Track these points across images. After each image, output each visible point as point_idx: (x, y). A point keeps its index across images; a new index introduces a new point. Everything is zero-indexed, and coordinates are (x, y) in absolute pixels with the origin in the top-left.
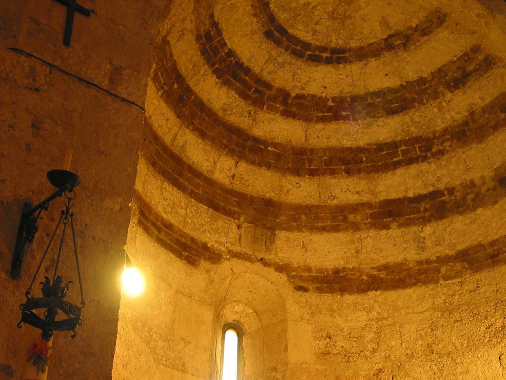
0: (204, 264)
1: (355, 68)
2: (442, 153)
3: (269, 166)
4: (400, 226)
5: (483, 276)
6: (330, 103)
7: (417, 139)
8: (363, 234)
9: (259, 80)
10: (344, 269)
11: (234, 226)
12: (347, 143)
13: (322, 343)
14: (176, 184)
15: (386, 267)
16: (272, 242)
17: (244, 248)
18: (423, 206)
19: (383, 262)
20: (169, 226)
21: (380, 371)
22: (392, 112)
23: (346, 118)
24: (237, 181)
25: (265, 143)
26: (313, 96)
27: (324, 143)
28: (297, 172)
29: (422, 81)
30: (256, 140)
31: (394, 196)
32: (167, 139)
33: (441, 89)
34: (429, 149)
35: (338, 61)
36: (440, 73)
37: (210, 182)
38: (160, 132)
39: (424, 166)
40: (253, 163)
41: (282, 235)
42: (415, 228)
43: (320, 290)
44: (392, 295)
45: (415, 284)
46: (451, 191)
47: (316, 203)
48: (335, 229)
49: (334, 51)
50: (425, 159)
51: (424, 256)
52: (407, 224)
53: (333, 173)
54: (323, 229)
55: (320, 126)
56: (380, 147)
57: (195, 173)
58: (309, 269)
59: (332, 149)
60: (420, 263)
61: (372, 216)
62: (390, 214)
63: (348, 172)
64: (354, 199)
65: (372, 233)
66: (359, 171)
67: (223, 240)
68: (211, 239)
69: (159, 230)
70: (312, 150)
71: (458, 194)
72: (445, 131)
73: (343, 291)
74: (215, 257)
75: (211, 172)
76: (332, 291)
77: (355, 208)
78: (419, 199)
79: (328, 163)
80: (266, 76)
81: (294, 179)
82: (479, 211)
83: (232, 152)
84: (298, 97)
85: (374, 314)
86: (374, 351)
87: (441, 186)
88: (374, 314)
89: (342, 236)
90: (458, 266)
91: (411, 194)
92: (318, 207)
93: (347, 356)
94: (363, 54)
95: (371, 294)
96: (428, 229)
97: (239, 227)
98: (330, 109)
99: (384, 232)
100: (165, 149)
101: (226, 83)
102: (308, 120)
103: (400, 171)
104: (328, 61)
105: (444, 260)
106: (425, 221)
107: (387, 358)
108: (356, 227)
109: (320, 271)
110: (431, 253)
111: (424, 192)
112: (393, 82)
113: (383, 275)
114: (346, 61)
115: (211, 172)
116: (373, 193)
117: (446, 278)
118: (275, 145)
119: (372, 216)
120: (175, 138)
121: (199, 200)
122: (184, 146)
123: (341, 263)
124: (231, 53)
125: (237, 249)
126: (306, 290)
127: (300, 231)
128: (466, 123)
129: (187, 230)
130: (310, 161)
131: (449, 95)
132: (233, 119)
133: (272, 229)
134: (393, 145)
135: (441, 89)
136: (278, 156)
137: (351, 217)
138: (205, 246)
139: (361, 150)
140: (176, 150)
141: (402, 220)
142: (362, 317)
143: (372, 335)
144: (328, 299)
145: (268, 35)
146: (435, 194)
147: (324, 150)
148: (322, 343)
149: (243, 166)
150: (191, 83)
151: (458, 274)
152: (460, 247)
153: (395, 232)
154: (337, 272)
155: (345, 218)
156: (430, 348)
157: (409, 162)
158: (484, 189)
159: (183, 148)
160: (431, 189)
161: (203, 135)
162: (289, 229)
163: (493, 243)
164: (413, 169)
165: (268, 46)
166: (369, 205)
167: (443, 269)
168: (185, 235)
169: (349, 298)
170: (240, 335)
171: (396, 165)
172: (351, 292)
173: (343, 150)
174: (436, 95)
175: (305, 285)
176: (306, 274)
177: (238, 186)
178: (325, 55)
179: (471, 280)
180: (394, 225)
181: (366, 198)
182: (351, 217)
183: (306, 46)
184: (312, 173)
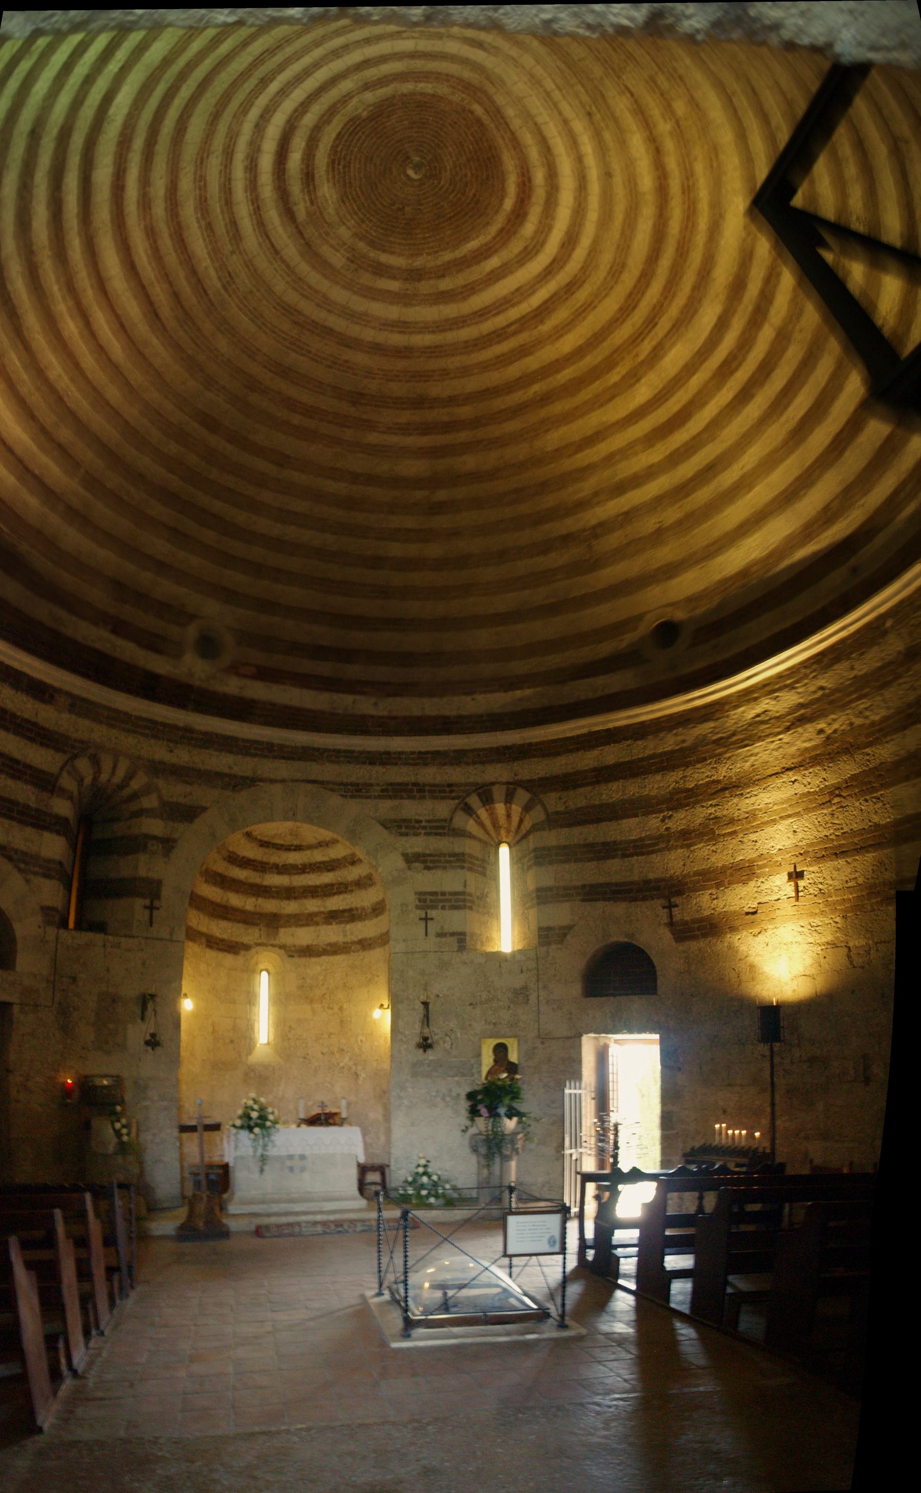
0: (243, 952)
1: (308, 852)
2: (352, 891)
3: (273, 897)
4: (337, 923)
5: (366, 953)
6: (300, 866)
7: (341, 884)
8: (320, 927)
9: (262, 863)
10: (311, 945)
11: (257, 930)
12: (311, 883)
13: (301, 982)
14: (226, 919)
15: (330, 944)
16: (277, 934)
17: (263, 940)
18: (346, 914)
19: (328, 941)
20: (223, 940)
21: (325, 994)
22: (329, 871)
23: (308, 873)
24: (258, 908)
25: (270, 887)
26: (291, 864)
27: (300, 884)
28: (288, 898)
29: (338, 860)
30: (266, 887)
31: (334, 908)
32: (218, 900)
33: (347, 865)
34: (346, 888)
35: (300, 850)
36: (344, 858)
37: (243, 912)
38: (214, 899)
39: (346, 896)
40: (265, 897)
41: (282, 931)
42: (343, 925)
43: (300, 956)
44: (332, 958)
45: (341, 953)
46: (357, 909)
47: (297, 912)
48: (307, 925)
49: (296, 846)
50: (346, 892)
51: (345, 940)
52: (340, 923)
53: (305, 897)
54: (302, 925)
55: (296, 877)
56: (326, 886)
57: (235, 910)
58: (295, 946)
59: (304, 887)
60: (344, 943)
61: (325, 918)
62: (332, 917)
63: (313, 897)
64: (316, 909)
65: (325, 927)
66: (318, 896)
67: (251, 938)
68: (246, 940)
69: (218, 944)
70: (294, 888)
71: (359, 911)
72: (352, 882)
73: (310, 956)
74: (247, 948)
75: (244, 907)
76: (305, 956)
77: (316, 914)
78: (344, 911)
79: (304, 892)
80: (265, 860)
81: (286, 902)
82: (367, 922)
83: (254, 895)
84: (283, 866)
85: (324, 967)
86: (323, 985)
87: (353, 906)
88: (324, 967)
89: (311, 929)
90: (358, 947)
91: (341, 908)
92: (299, 914)
93: (311, 988)
94: (310, 847)
95: (323, 957)
96: (348, 927)
97: (260, 930)
98: (300, 869)
99: (330, 927)
100: (218, 905)
101: (245, 868)
102: (289, 874)
103: (336, 897)
104: (295, 850)
105: (353, 943)
106: (347, 922)
107: (328, 988)
108: (317, 924)
109: (301, 946)
110: (349, 939)
111: (347, 908)
112: (326, 859)
113: (328, 948)
114: (303, 850)
115: (244, 907)
116: (325, 907)
117: (354, 952)
118: (275, 887)
119: (325, 918)
120: (222, 898)
121: (239, 922)
122: (228, 899)
123: (310, 942)
124: (243, 858)
125: (260, 941)
126: (292, 956)
127: (290, 926)
128: (359, 880)
129: (233, 939)
130: (294, 893)
131: (350, 867)
132: (252, 881)
133: (277, 928)
134: (332, 885)
135: (347, 865)
136: (278, 892)
137: (315, 919)
138: (242, 944)
139: (316, 887)
140: (224, 903)
141: (337, 921)
142: (318, 968)
143: (322, 978)
144: (303, 960)
145: (261, 846)
146: (351, 910)
147: (301, 887)
148: (301, 982)
149: (260, 900)
150: (226, 874)
151: (358, 951)
152: (360, 937)
153: (334, 927)
154: (308, 946)
155: (312, 920)
156: (345, 985)
157: (340, 893)
158: (368, 911)
159: (227, 901)
160: (349, 907)
161: (237, 892)
162: (285, 927)
163: (370, 939)
164: (342, 897)
165: (261, 849)
166: (323, 913)
167: (353, 948)
168: (232, 942)
169: (313, 960)
170: (269, 973)
171: (334, 894)
172: (314, 956)
173: (309, 887)
174: (345, 867)
175: (293, 954)
176: (293, 949)
177: (258, 910)
178: (292, 848)
179: (363, 954)
180: (334, 923)
181: (322, 909)
182: (315, 919)
183: (282, 845)
184: (295, 898)
